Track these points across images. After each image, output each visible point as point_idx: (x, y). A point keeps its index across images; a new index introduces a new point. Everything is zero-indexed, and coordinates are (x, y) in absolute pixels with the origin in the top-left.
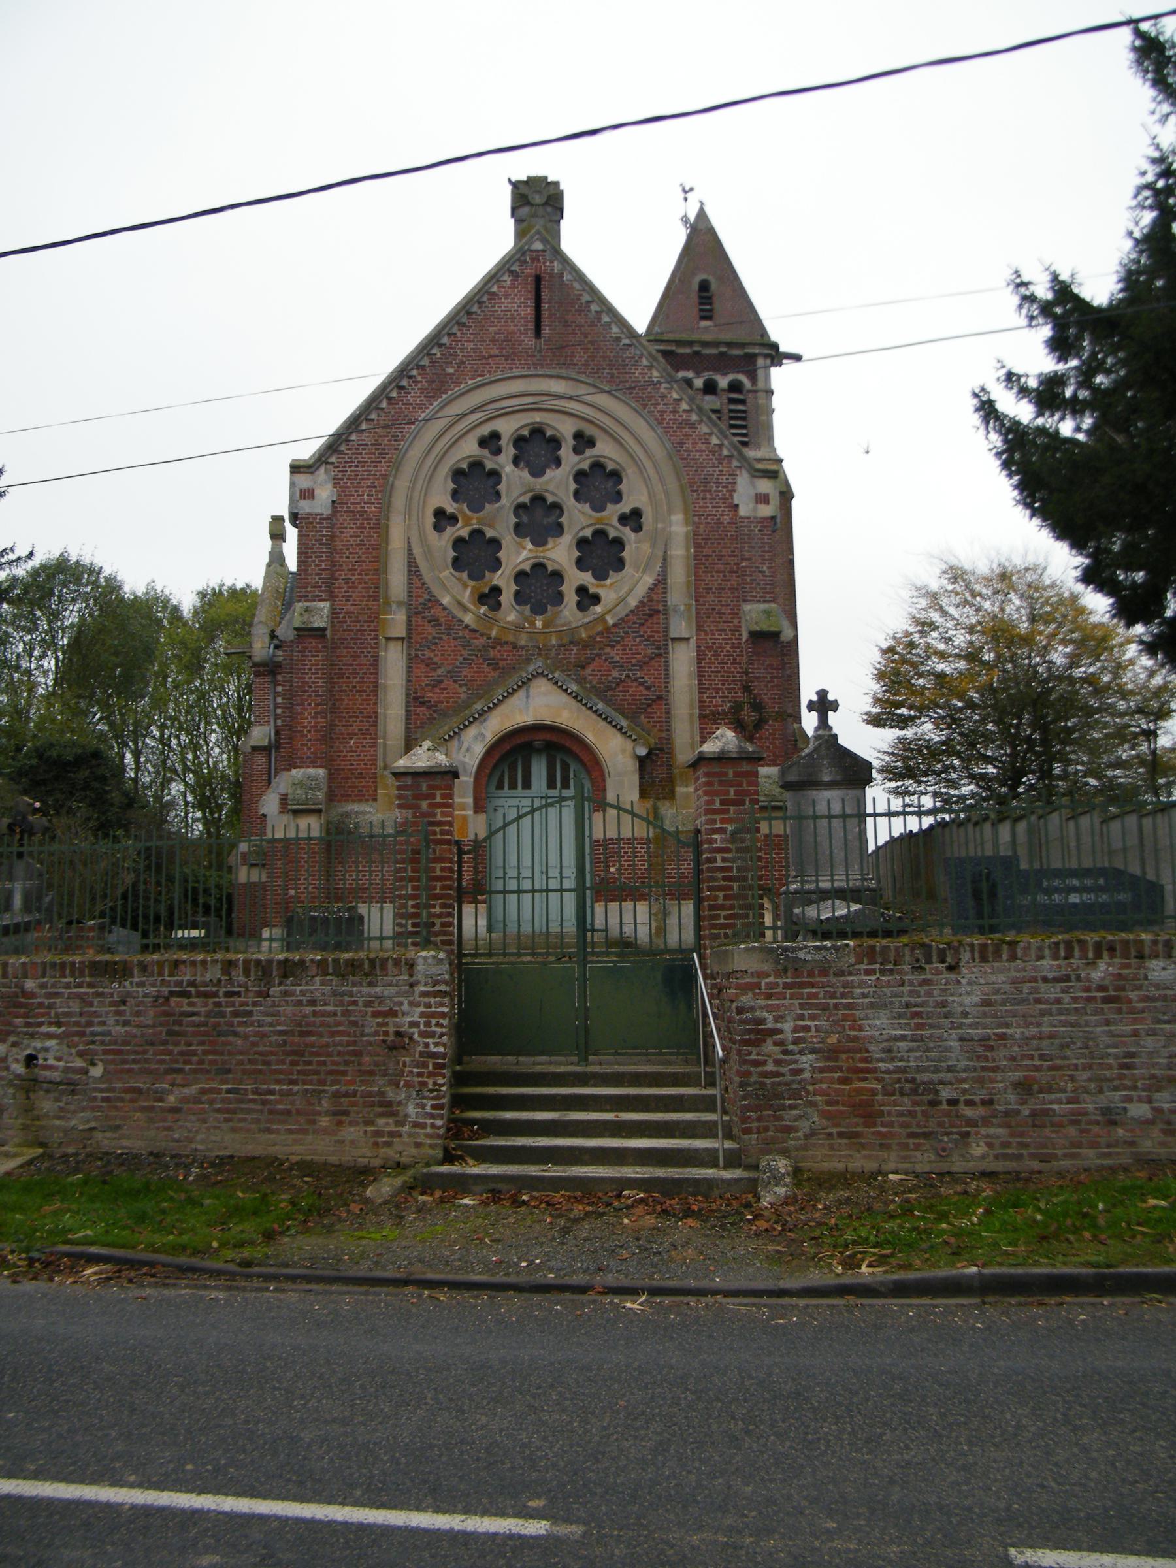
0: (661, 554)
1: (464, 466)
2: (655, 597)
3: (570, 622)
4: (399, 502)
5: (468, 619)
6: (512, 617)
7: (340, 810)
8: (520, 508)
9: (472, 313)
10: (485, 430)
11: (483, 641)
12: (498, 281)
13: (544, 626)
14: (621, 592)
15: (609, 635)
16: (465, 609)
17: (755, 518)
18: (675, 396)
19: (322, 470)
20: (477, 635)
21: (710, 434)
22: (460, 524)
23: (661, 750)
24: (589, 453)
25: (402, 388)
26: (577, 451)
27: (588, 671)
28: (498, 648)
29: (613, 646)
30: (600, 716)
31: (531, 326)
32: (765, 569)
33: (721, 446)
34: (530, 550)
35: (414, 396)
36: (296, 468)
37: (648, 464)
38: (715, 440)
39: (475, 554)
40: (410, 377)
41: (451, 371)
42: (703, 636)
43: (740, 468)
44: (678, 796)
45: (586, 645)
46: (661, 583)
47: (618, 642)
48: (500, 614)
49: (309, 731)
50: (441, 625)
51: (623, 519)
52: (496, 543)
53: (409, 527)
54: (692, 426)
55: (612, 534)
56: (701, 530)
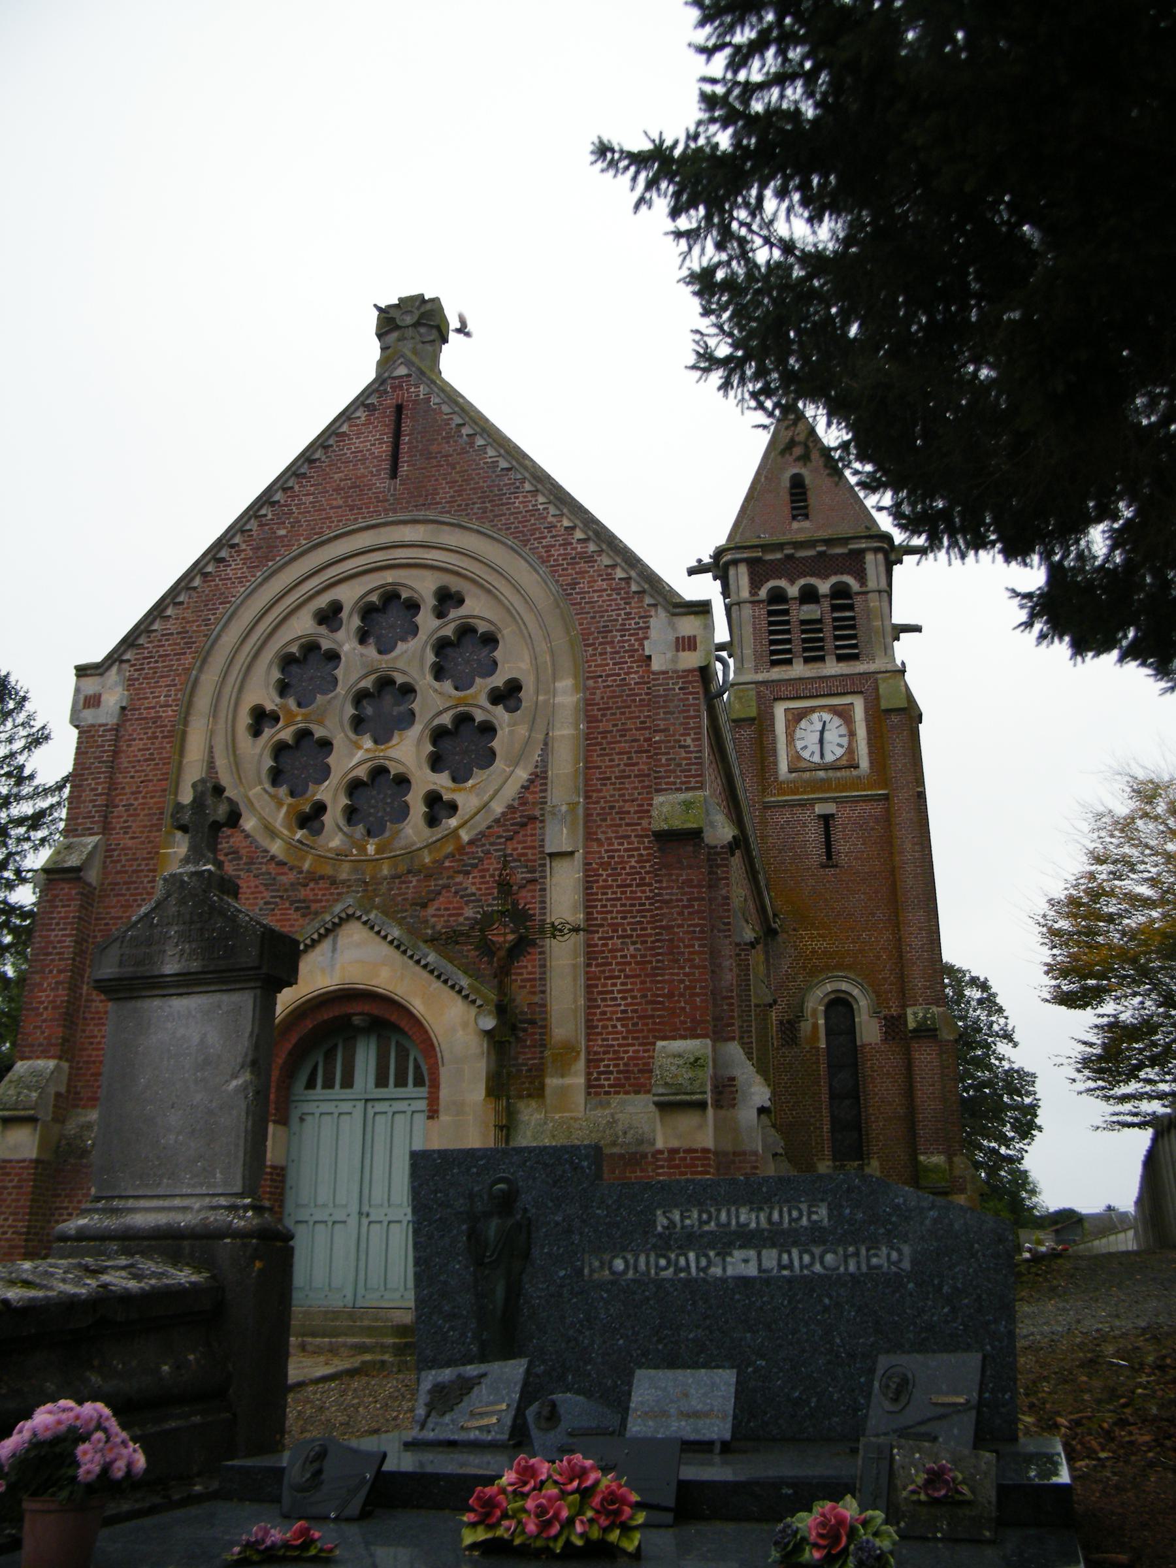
0: (541, 737)
1: (294, 649)
2: (530, 798)
3: (414, 844)
4: (203, 702)
5: (276, 848)
6: (336, 842)
7: (83, 1119)
8: (360, 697)
9: (315, 461)
10: (323, 601)
11: (292, 877)
12: (349, 419)
13: (378, 851)
14: (482, 798)
15: (463, 857)
16: (273, 834)
17: (675, 671)
18: (566, 523)
19: (114, 669)
20: (286, 869)
21: (614, 566)
22: (280, 725)
23: (533, 1022)
24: (453, 614)
25: (222, 560)
26: (440, 614)
27: (431, 910)
28: (312, 885)
29: (467, 873)
30: (432, 972)
31: (386, 465)
32: (689, 741)
33: (628, 580)
34: (367, 750)
35: (235, 568)
36: (82, 671)
37: (529, 618)
38: (620, 574)
39: (298, 760)
40: (232, 546)
41: (282, 532)
42: (595, 848)
43: (655, 605)
44: (548, 1091)
45: (429, 874)
46: (539, 778)
47: (475, 866)
48: (321, 839)
49: (46, 1008)
50: (240, 858)
51: (497, 697)
52: (326, 745)
53: (212, 733)
54: (590, 559)
55: (479, 716)
56: (597, 697)
